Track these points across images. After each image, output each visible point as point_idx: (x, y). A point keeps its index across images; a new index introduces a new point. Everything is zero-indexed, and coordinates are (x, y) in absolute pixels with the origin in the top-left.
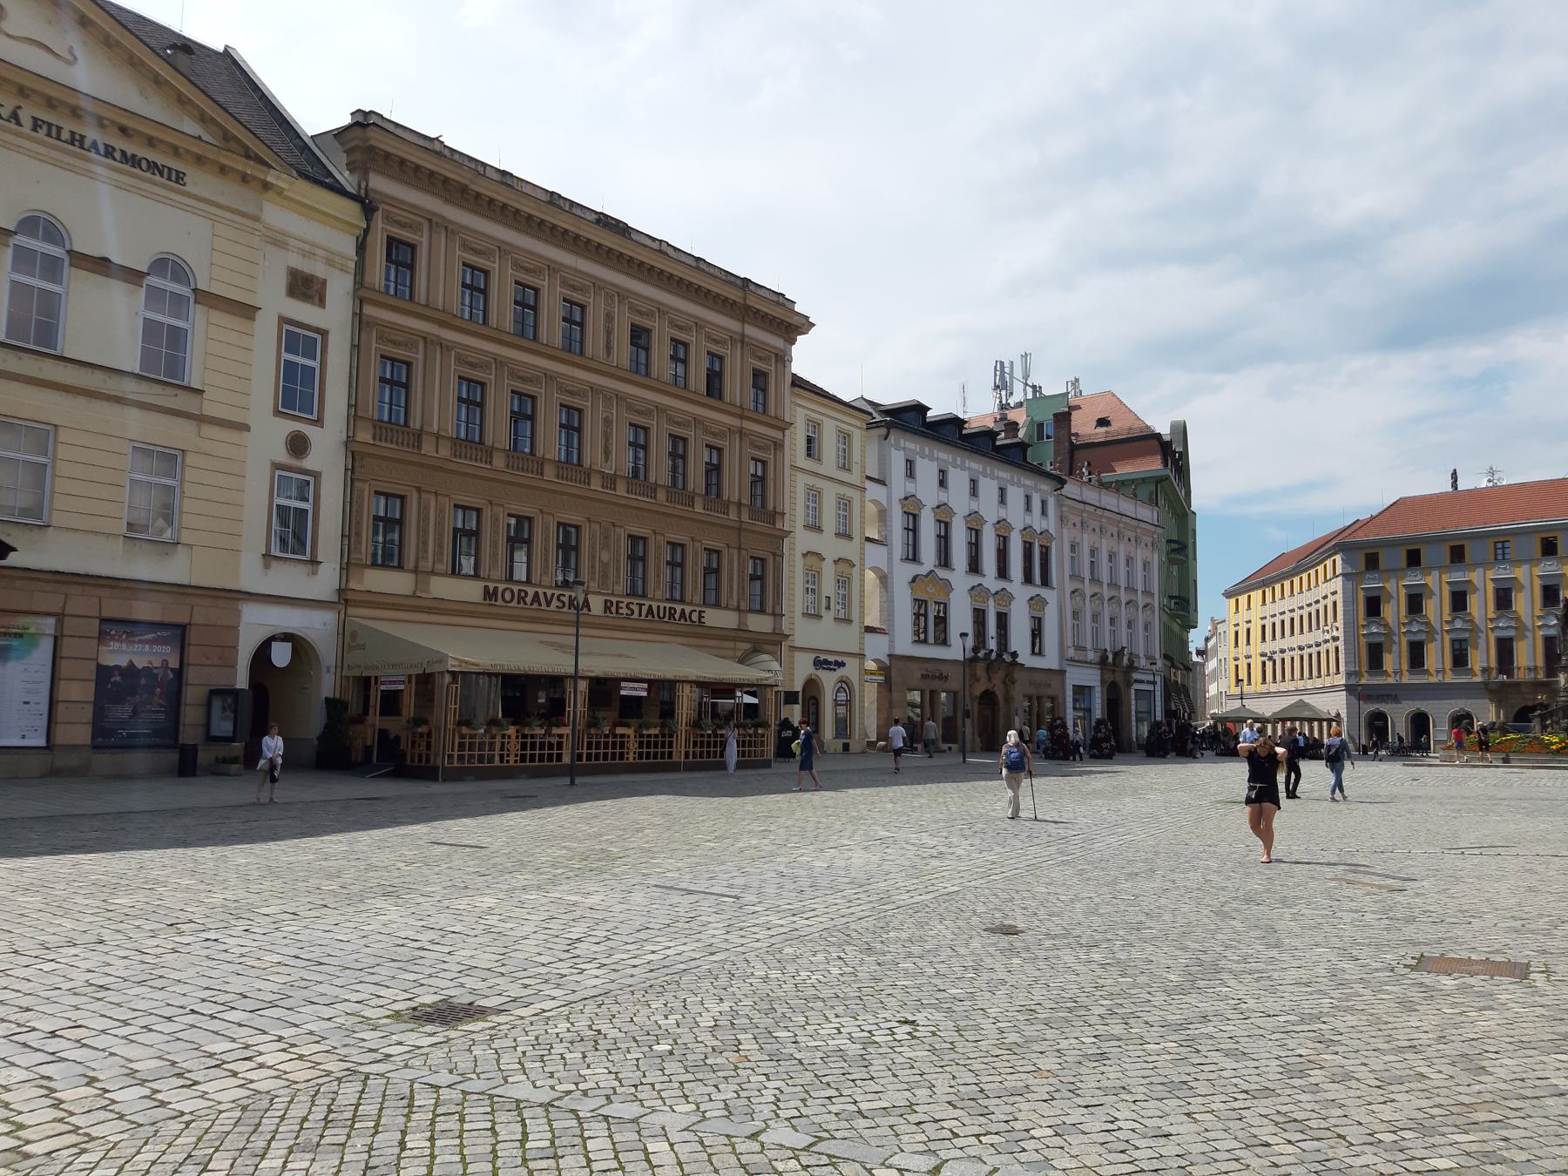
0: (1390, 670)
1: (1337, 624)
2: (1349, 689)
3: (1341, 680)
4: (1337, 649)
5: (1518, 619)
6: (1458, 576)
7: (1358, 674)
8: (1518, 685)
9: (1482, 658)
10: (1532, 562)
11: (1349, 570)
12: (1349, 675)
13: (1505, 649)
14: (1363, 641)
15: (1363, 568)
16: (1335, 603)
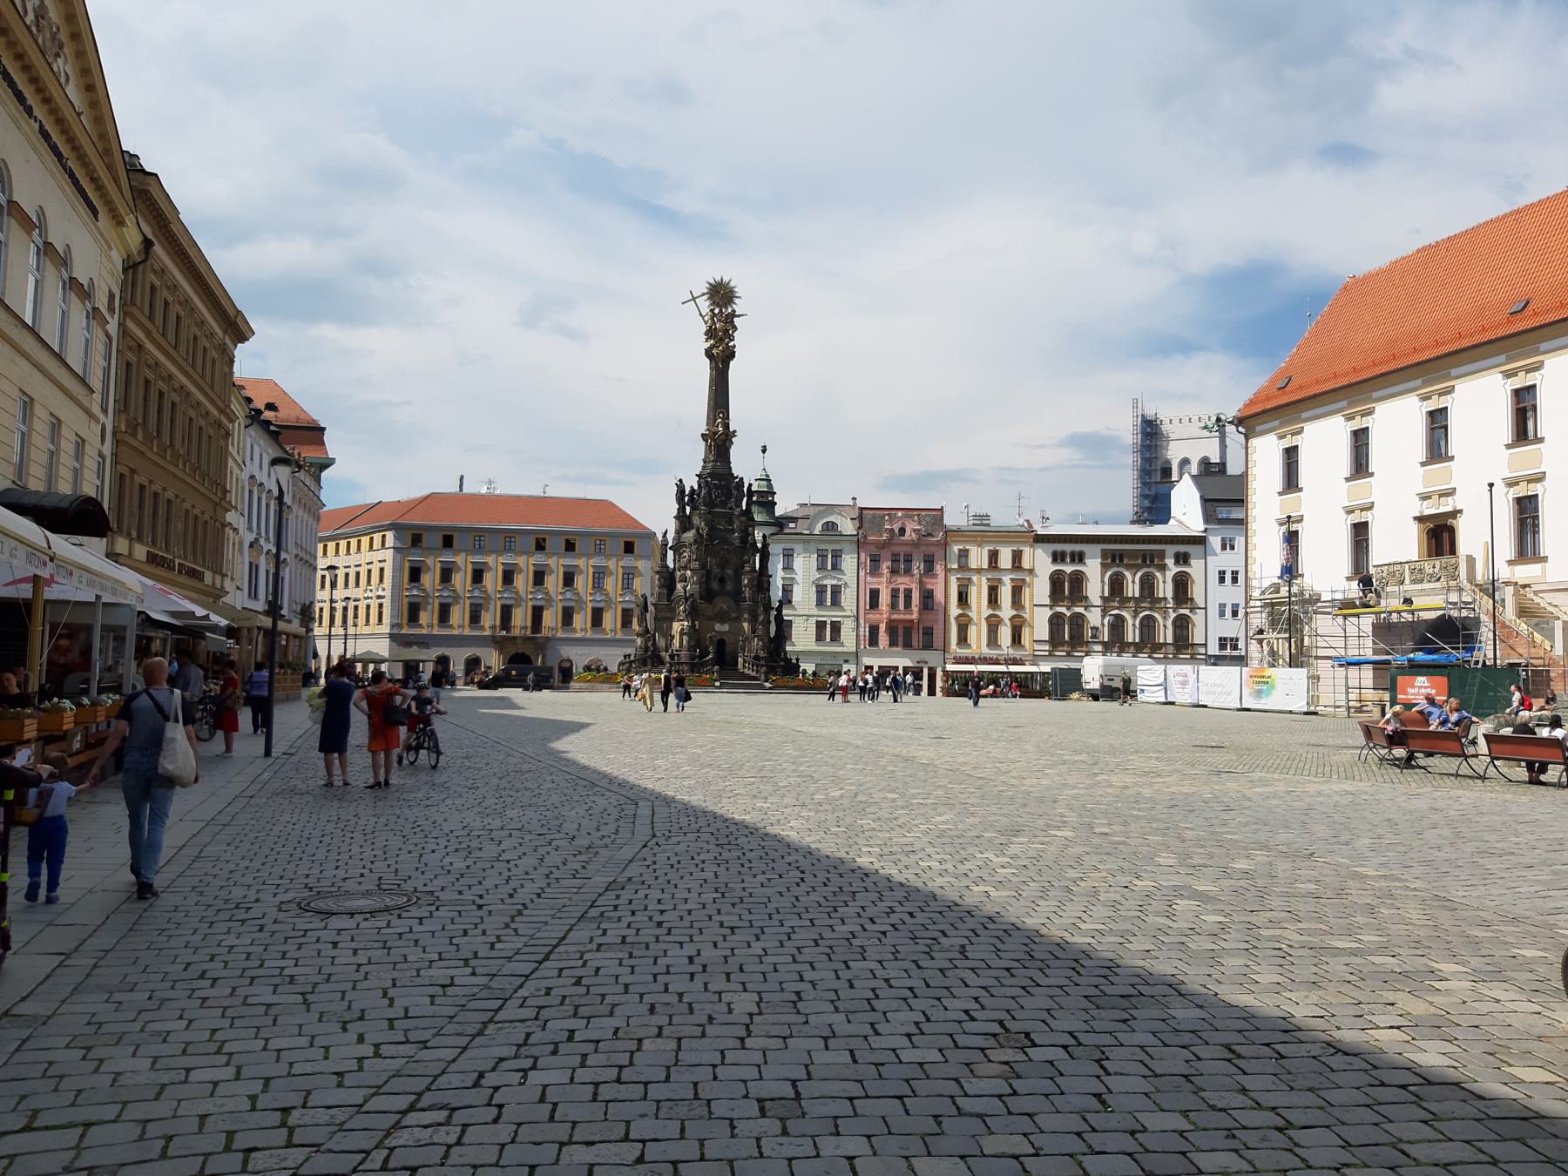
0: (424, 624)
1: (384, 586)
2: (392, 637)
3: (385, 629)
4: (381, 605)
5: (517, 593)
6: (478, 559)
7: (399, 626)
8: (514, 638)
9: (490, 619)
10: (530, 554)
11: (399, 545)
12: (393, 626)
13: (506, 612)
14: (406, 601)
15: (410, 542)
16: (382, 570)
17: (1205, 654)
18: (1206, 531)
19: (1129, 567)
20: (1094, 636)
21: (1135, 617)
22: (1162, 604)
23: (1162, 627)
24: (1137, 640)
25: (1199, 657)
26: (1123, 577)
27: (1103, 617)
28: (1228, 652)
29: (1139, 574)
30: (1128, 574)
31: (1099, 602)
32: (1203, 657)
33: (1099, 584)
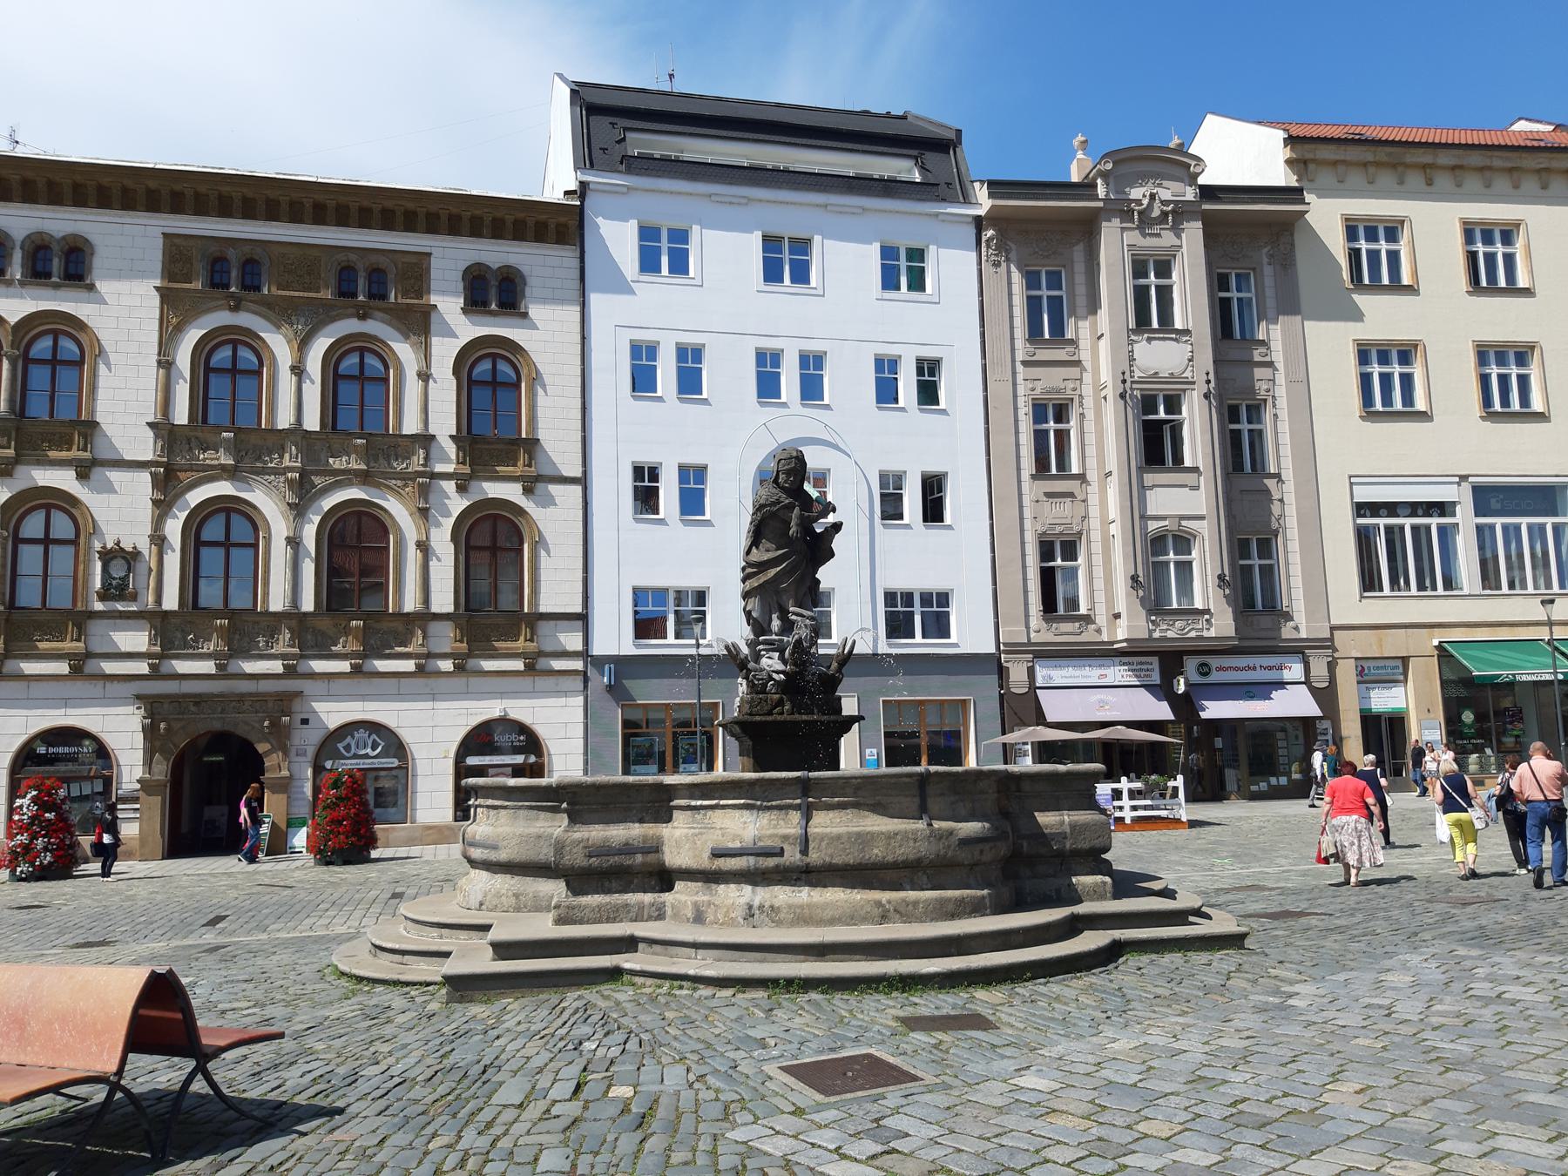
17: (585, 654)
18: (583, 189)
19: (280, 313)
20: (115, 590)
21: (298, 510)
22: (416, 462)
23: (412, 556)
24: (308, 604)
25: (558, 664)
26: (261, 351)
27: (163, 507)
28: (670, 644)
29: (321, 345)
30: (279, 345)
31: (143, 446)
32: (578, 665)
33: (150, 375)
